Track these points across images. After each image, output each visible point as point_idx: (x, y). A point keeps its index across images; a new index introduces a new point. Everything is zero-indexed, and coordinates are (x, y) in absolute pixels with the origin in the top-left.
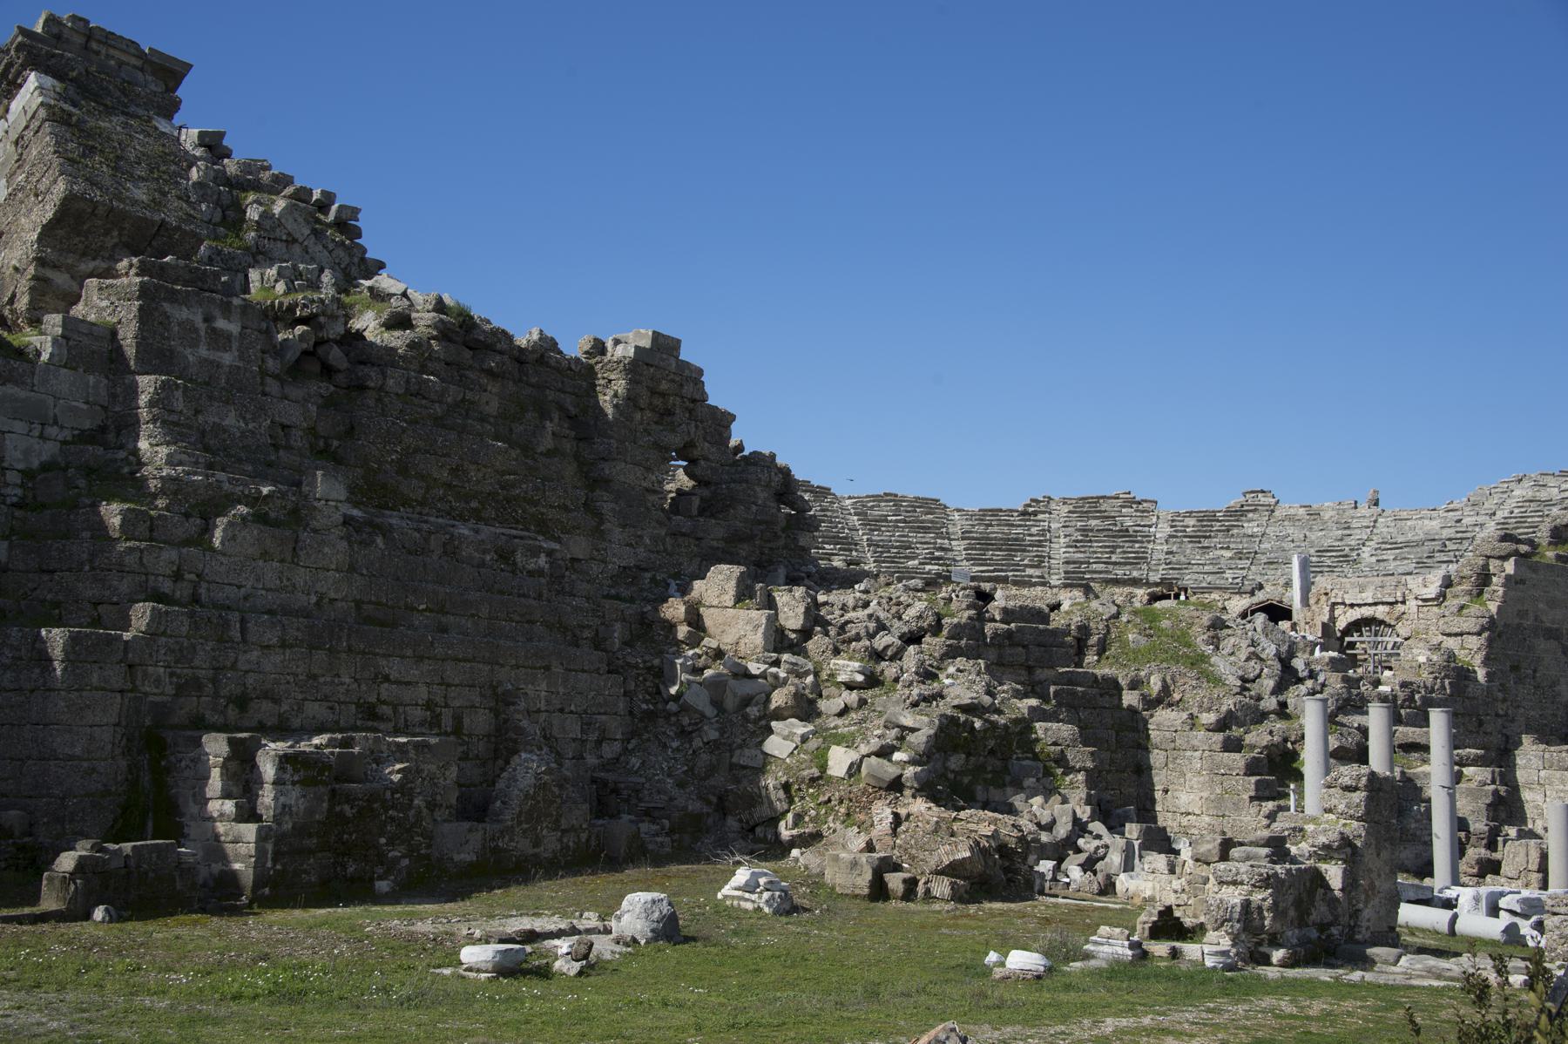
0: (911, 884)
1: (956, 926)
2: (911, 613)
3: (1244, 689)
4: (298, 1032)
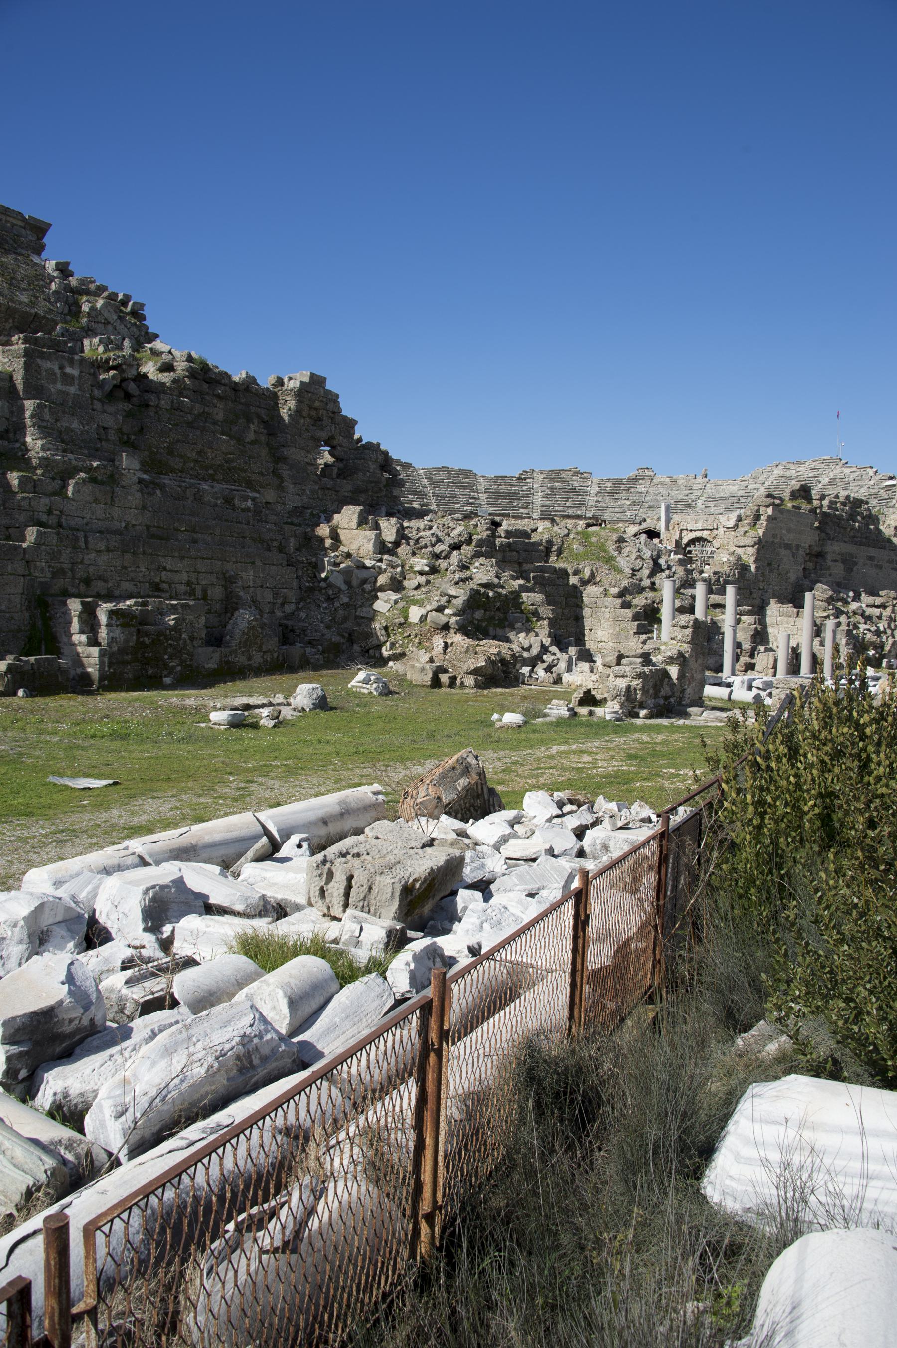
0: (453, 680)
1: (477, 701)
2: (455, 533)
3: (633, 575)
4: (125, 754)
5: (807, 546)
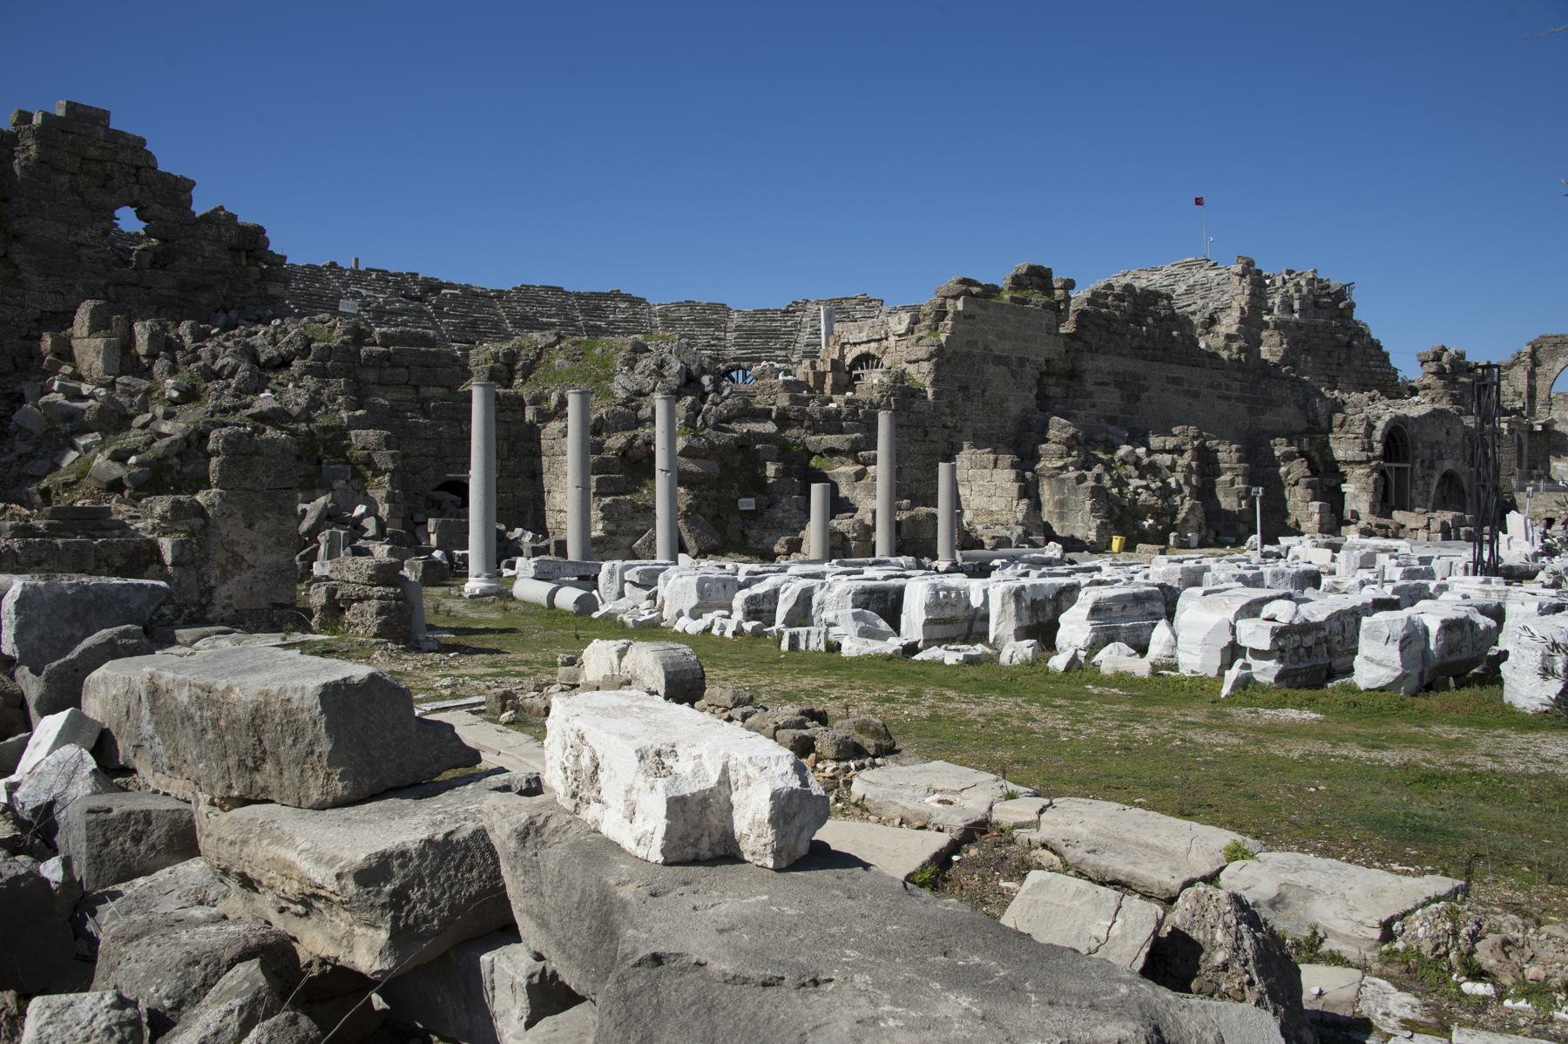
5: (1041, 360)
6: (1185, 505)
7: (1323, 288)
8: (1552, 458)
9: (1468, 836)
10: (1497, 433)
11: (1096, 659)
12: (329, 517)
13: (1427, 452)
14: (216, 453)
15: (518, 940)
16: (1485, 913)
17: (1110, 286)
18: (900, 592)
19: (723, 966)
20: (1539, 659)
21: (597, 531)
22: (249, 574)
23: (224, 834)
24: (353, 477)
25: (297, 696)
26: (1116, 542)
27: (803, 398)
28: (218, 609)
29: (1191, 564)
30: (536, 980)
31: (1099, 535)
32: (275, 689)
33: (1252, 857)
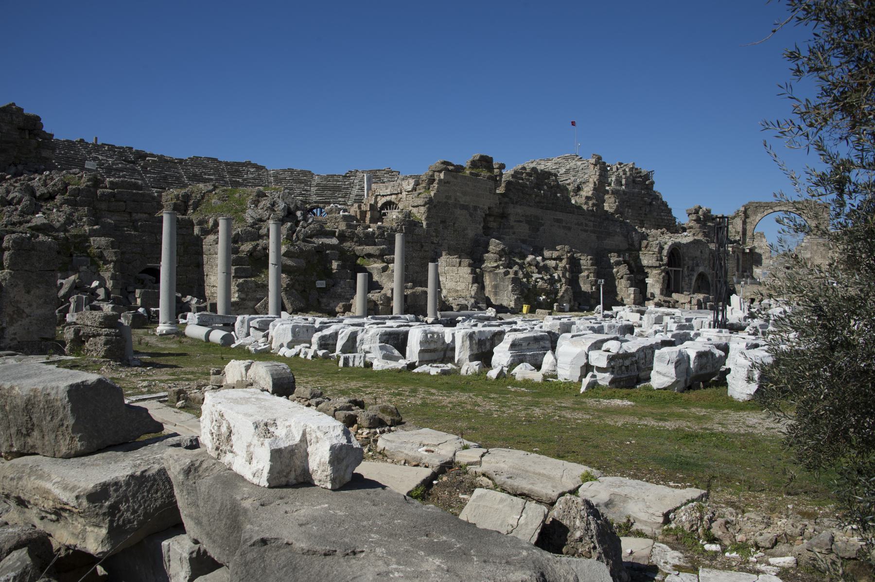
5: (486, 207)
6: (562, 288)
7: (637, 173)
8: (754, 267)
9: (708, 467)
10: (727, 252)
11: (513, 372)
12: (76, 288)
13: (691, 262)
14: (8, 249)
15: (184, 532)
16: (717, 507)
17: (524, 168)
18: (406, 334)
19: (302, 545)
20: (746, 373)
21: (235, 298)
22: (27, 320)
23: (7, 474)
24: (91, 265)
25: (53, 392)
26: (525, 308)
27: (353, 225)
28: (8, 341)
29: (565, 320)
30: (194, 555)
31: (516, 304)
32: (40, 387)
33: (596, 479)
